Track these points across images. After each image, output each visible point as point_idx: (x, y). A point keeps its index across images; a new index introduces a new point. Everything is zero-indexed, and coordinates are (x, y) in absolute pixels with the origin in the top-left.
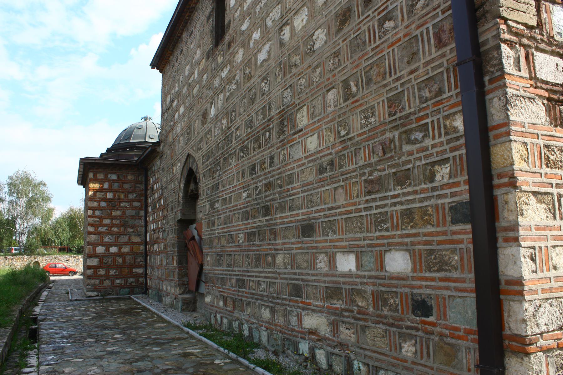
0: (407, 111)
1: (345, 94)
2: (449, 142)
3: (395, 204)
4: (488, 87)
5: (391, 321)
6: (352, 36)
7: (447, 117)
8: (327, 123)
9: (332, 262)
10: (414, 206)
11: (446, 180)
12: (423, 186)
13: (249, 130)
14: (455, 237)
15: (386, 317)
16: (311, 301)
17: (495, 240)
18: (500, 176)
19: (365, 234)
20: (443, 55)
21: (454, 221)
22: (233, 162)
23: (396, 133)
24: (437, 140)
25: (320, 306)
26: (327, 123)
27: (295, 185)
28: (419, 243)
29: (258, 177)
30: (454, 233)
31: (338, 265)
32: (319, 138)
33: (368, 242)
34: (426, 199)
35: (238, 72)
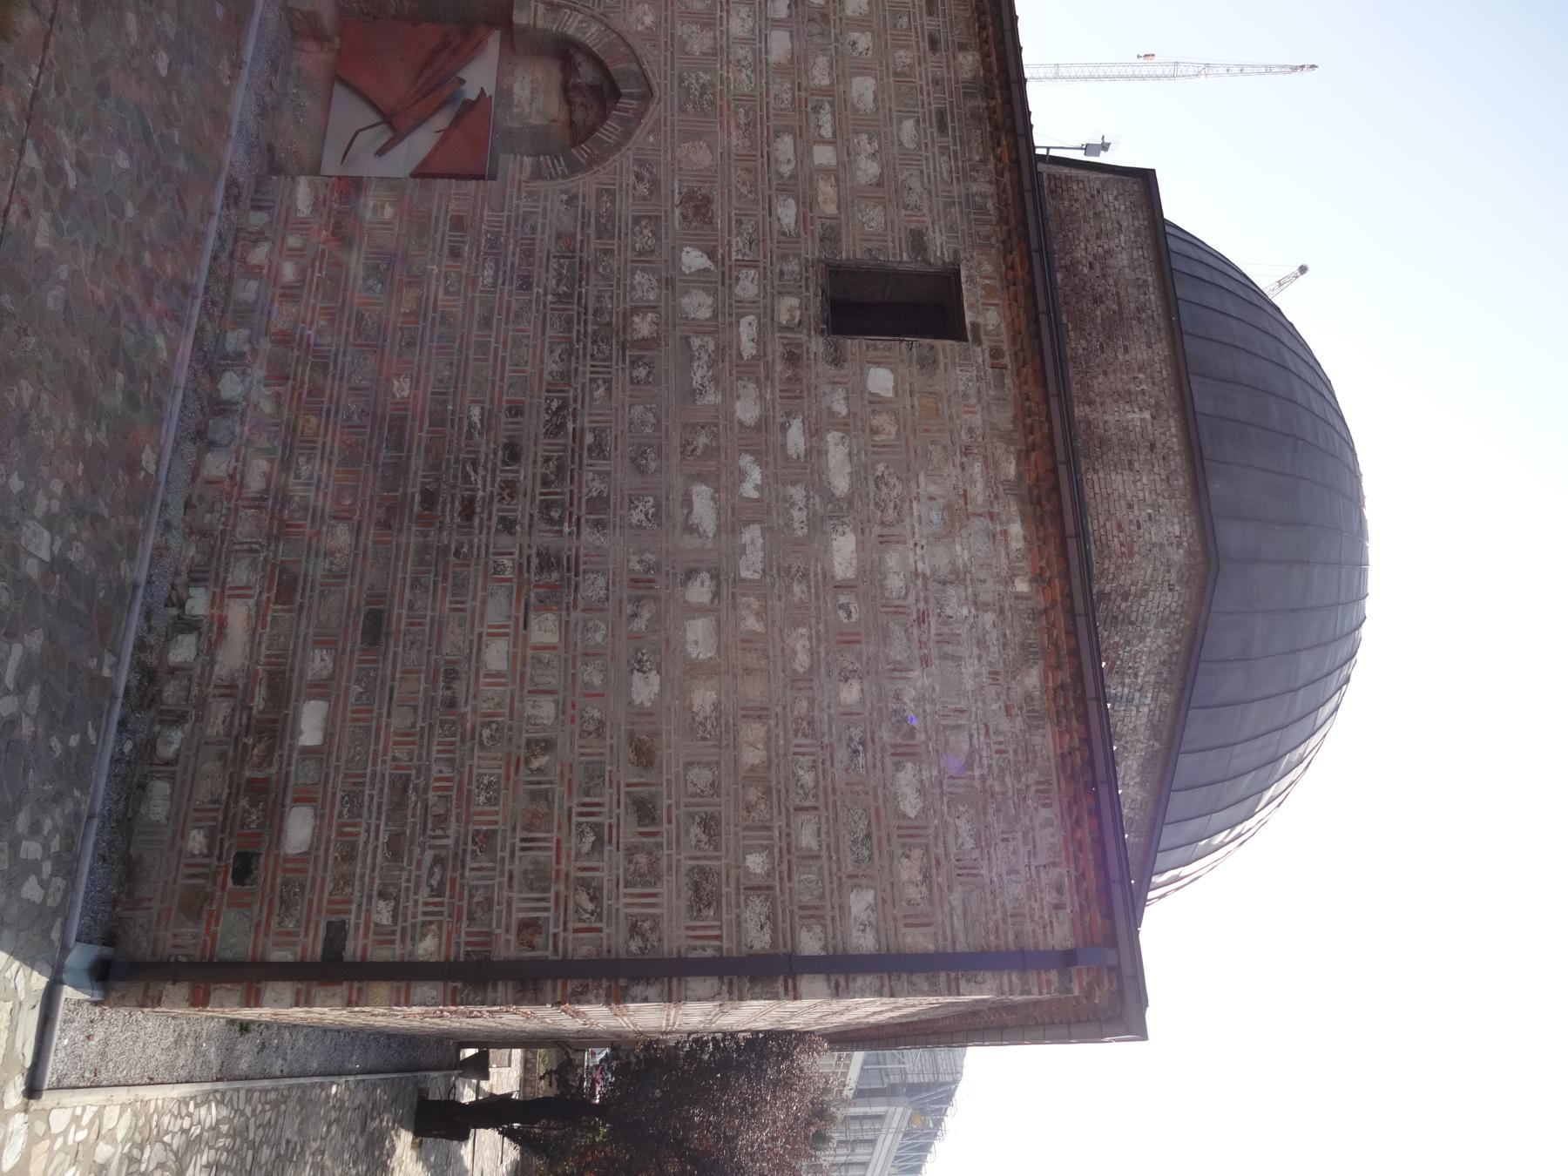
0: (470, 864)
1: (537, 742)
2: (414, 925)
3: (368, 831)
4: (451, 985)
5: (231, 812)
6: (608, 768)
7: (440, 928)
8: (512, 697)
9: (320, 689)
10: (359, 865)
11: (375, 918)
12: (377, 881)
13: (589, 439)
14: (312, 926)
15: (236, 803)
16: (268, 629)
17: (300, 980)
18: (360, 990)
19: (342, 770)
20: (507, 931)
21: (330, 924)
22: (552, 366)
23: (450, 842)
24: (421, 909)
25: (259, 654)
26: (512, 697)
27: (448, 598)
28: (315, 870)
29: (494, 471)
30: (317, 924)
31: (313, 703)
32: (499, 675)
33: (332, 775)
34: (362, 885)
35: (719, 400)
